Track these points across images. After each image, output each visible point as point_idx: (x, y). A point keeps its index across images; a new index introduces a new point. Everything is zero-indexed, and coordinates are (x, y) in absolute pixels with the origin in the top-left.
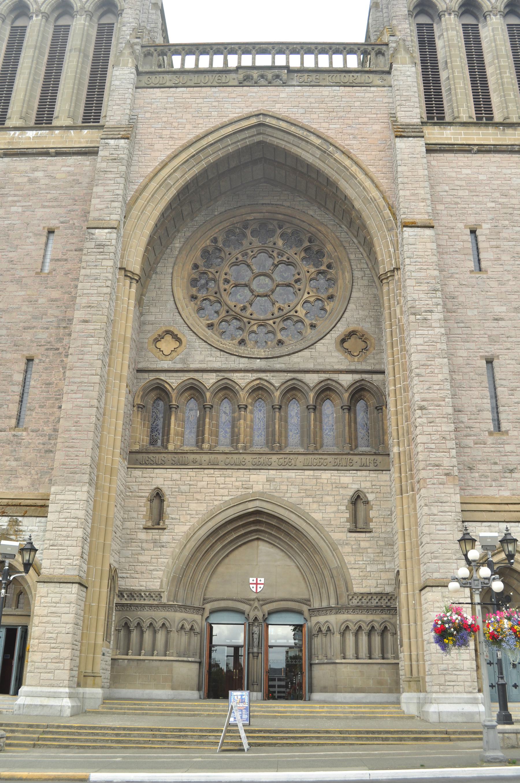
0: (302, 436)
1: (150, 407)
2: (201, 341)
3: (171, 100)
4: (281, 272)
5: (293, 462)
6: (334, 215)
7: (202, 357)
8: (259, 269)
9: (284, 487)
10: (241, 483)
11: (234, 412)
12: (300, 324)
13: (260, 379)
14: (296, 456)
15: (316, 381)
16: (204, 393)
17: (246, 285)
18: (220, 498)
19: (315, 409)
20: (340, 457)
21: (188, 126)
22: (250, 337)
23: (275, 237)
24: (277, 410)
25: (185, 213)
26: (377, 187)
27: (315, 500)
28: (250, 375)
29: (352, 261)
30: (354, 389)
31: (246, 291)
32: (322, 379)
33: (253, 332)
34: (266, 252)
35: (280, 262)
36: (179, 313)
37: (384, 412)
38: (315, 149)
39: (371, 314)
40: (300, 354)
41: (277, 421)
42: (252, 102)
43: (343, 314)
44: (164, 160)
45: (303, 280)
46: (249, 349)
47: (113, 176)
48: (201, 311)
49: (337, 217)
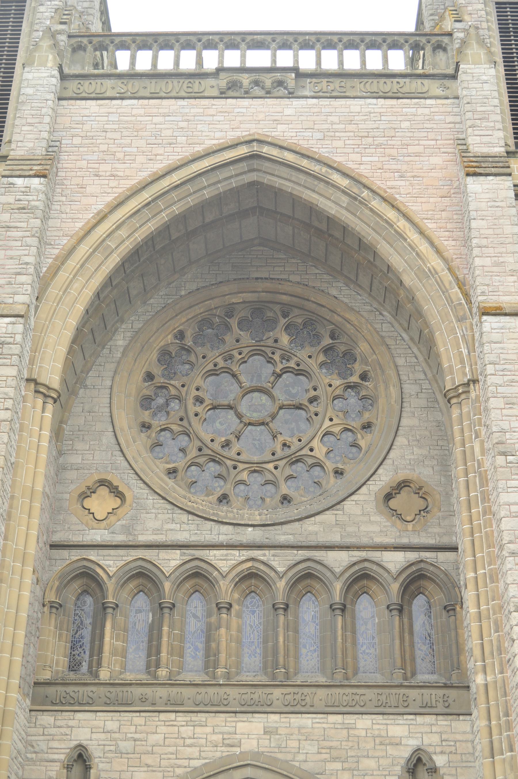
0: (323, 656)
1: (70, 606)
2: (157, 497)
3: (114, 118)
5: (308, 699)
6: (370, 295)
7: (157, 524)
8: (252, 381)
9: (293, 744)
10: (221, 736)
11: (209, 615)
12: (318, 469)
13: (252, 559)
14: (313, 690)
15: (345, 564)
16: (161, 583)
17: (230, 407)
18: (185, 763)
19: (343, 609)
20: (387, 691)
21: (141, 159)
22: (237, 490)
23: (276, 331)
24: (281, 612)
25: (134, 292)
26: (438, 252)
27: (346, 765)
28: (236, 553)
29: (400, 369)
30: (408, 577)
32: (355, 559)
33: (242, 482)
34: (261, 353)
35: (286, 370)
36: (122, 451)
37: (458, 616)
38: (339, 194)
39: (433, 452)
40: (318, 518)
41: (281, 630)
42: (241, 122)
43: (388, 452)
44: (101, 211)
46: (235, 511)
47: (20, 234)
48: (157, 449)
49: (374, 298)
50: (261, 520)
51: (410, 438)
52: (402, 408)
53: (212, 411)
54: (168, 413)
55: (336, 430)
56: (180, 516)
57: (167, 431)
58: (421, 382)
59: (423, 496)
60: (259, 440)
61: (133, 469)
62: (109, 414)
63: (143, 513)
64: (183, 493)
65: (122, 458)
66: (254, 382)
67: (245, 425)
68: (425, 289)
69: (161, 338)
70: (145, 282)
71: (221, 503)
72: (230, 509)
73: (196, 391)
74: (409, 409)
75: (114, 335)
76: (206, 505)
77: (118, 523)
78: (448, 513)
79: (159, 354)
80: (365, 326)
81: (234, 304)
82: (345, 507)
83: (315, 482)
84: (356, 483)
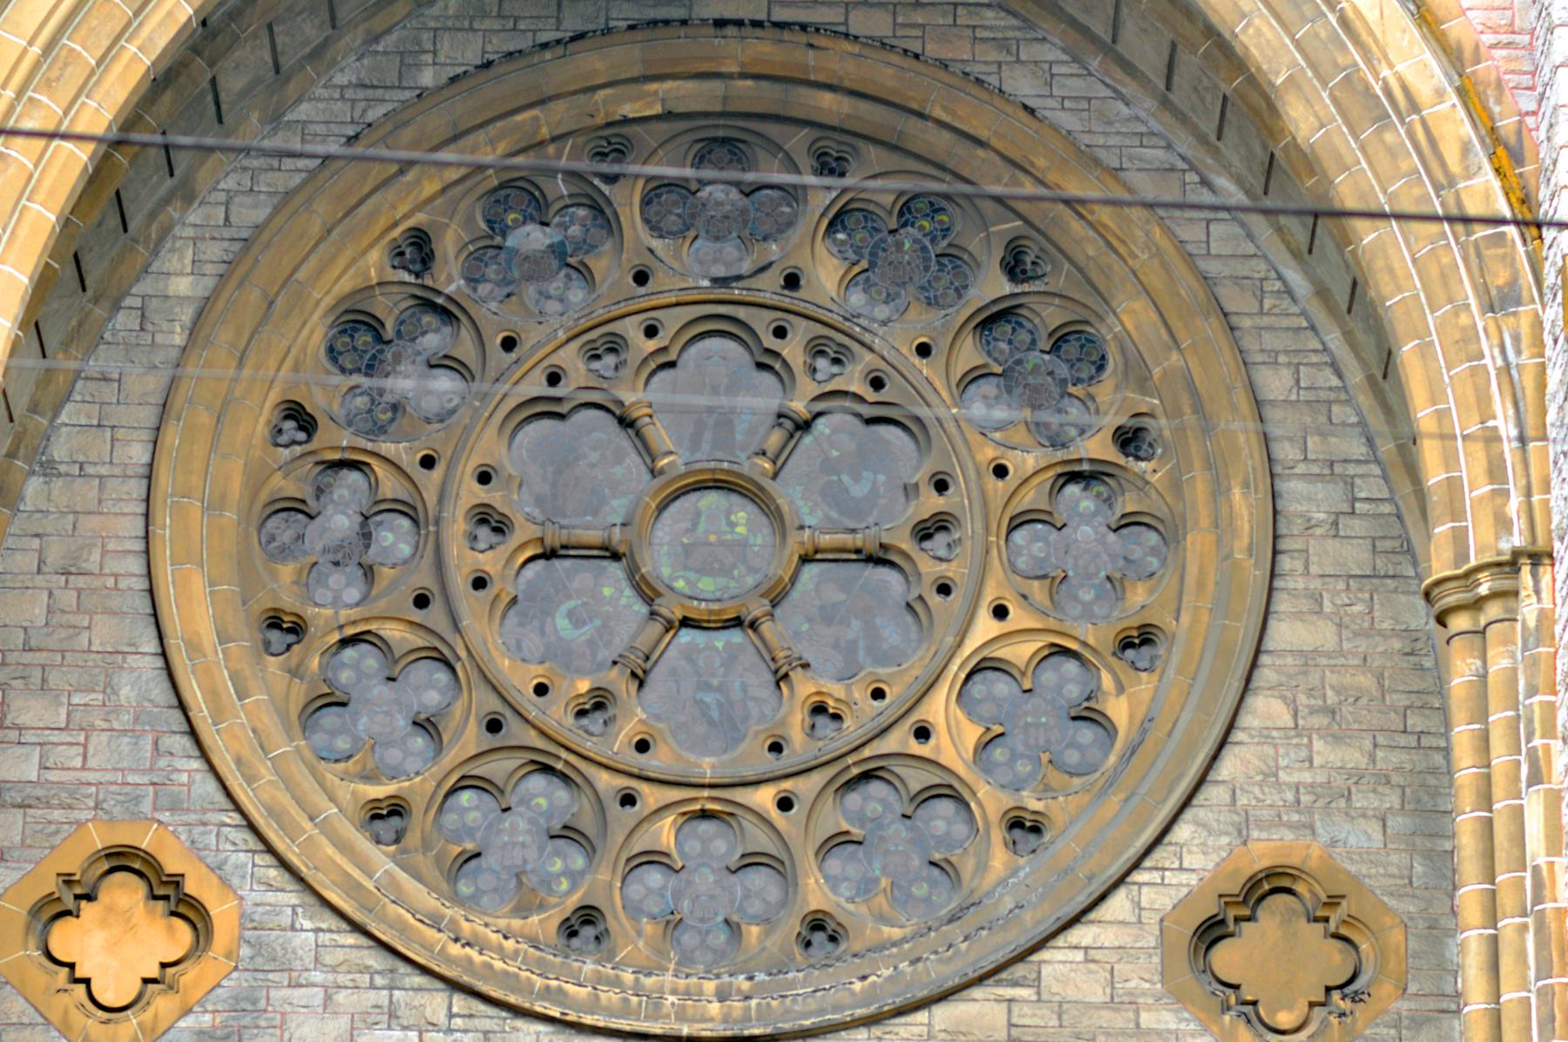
2: (330, 921)
4: (828, 466)
6: (1165, 103)
8: (695, 444)
12: (945, 807)
22: (635, 890)
25: (232, 84)
29: (1269, 413)
31: (612, 583)
33: (653, 858)
34: (736, 331)
39: (1388, 760)
43: (1215, 757)
45: (969, 528)
46: (628, 977)
48: (330, 718)
50: (725, 1019)
51: (1302, 699)
52: (1273, 575)
53: (541, 563)
54: (369, 572)
55: (1021, 652)
56: (419, 999)
57: (364, 647)
58: (1352, 470)
59: (1344, 931)
60: (719, 689)
61: (239, 809)
62: (143, 584)
63: (278, 986)
64: (429, 902)
65: (197, 764)
66: (706, 447)
67: (669, 626)
68: (1370, 163)
69: (342, 261)
70: (279, 40)
71: (575, 942)
72: (608, 970)
73: (477, 487)
74: (1300, 583)
75: (155, 253)
76: (517, 952)
77: (182, 1024)
78: (1432, 1004)
79: (331, 327)
80: (1139, 233)
81: (626, 121)
82: (1046, 970)
83: (932, 863)
84: (1090, 878)
